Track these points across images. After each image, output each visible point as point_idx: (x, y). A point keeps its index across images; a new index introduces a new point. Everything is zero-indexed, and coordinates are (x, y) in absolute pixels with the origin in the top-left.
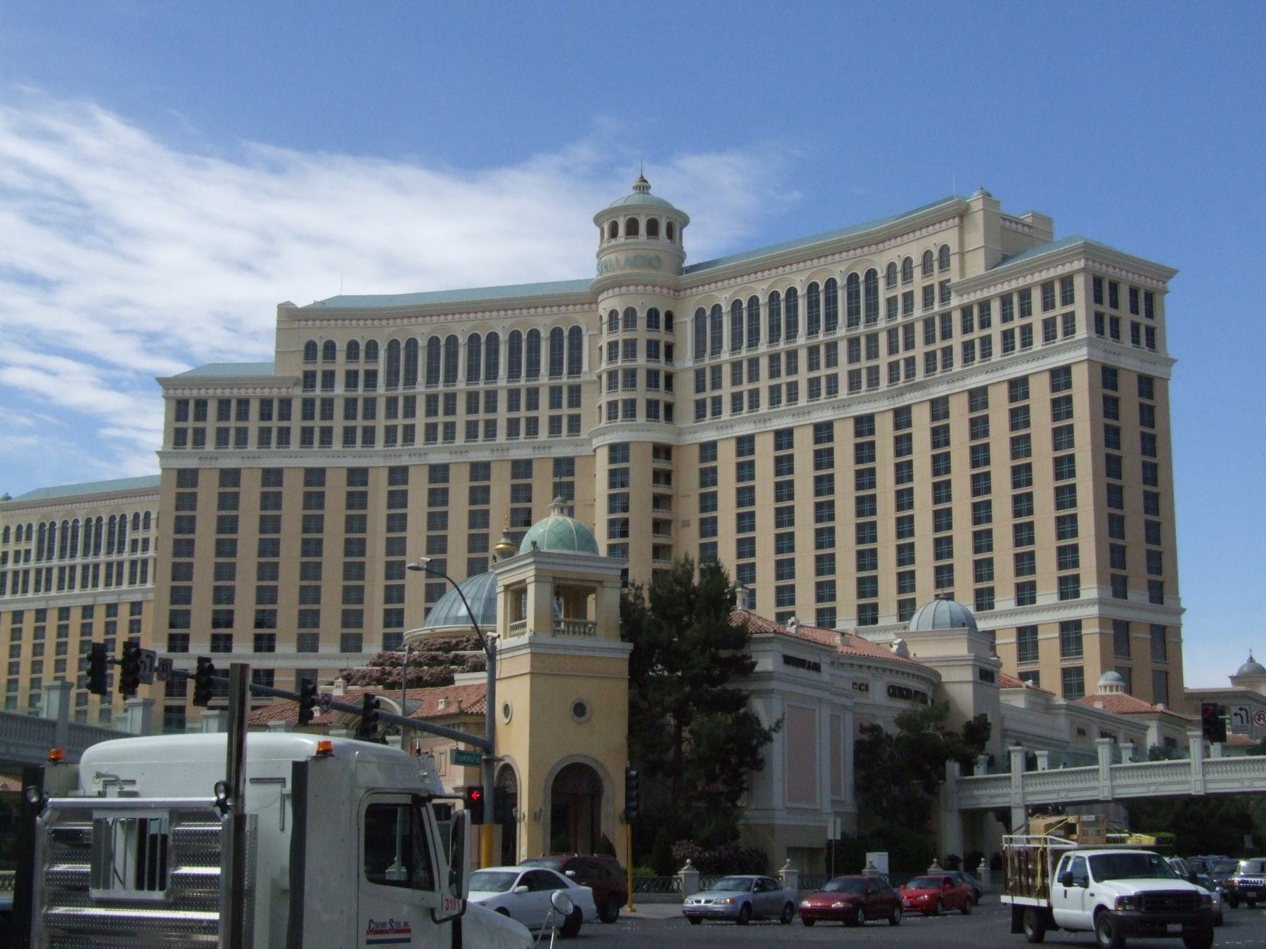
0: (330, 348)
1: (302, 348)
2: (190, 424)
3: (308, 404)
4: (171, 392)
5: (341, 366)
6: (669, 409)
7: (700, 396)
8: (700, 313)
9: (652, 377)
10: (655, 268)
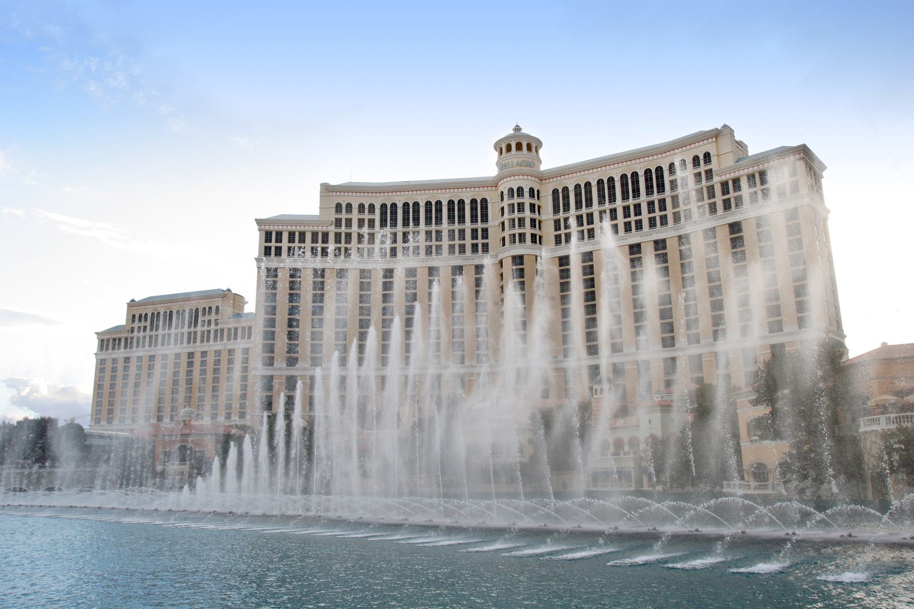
0: (349, 207)
1: (335, 206)
2: (273, 244)
3: (338, 236)
4: (263, 227)
5: (355, 216)
6: (540, 237)
7: (558, 233)
8: (555, 192)
9: (533, 221)
10: (531, 167)
